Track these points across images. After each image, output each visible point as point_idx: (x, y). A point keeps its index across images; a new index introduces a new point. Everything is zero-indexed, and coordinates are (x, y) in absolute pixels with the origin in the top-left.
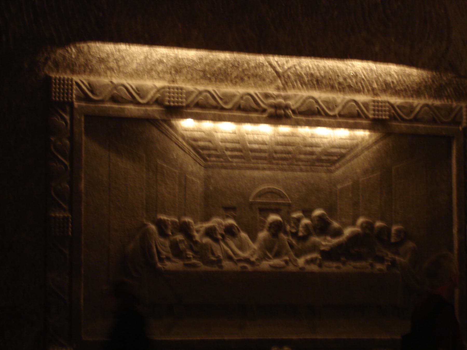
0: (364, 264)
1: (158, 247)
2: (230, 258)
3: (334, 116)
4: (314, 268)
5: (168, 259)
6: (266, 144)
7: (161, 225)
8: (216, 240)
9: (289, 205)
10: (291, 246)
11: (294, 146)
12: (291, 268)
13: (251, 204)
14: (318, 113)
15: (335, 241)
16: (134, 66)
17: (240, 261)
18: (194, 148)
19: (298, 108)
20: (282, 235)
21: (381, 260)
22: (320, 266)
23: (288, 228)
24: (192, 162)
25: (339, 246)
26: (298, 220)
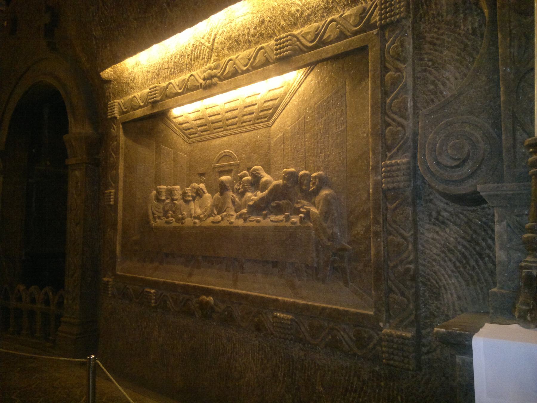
0: (281, 217)
1: (153, 209)
2: (190, 216)
3: (248, 71)
4: (240, 222)
5: (159, 218)
6: (219, 114)
7: (159, 193)
8: (187, 202)
9: (238, 165)
10: (233, 202)
11: (237, 109)
12: (224, 224)
13: (214, 168)
14: (235, 73)
15: (260, 194)
16: (140, 82)
17: (195, 218)
18: (181, 130)
19: (222, 74)
20: (230, 193)
21: (297, 211)
22: (245, 220)
23: (236, 186)
24: (181, 141)
25: (262, 199)
26: (241, 177)
